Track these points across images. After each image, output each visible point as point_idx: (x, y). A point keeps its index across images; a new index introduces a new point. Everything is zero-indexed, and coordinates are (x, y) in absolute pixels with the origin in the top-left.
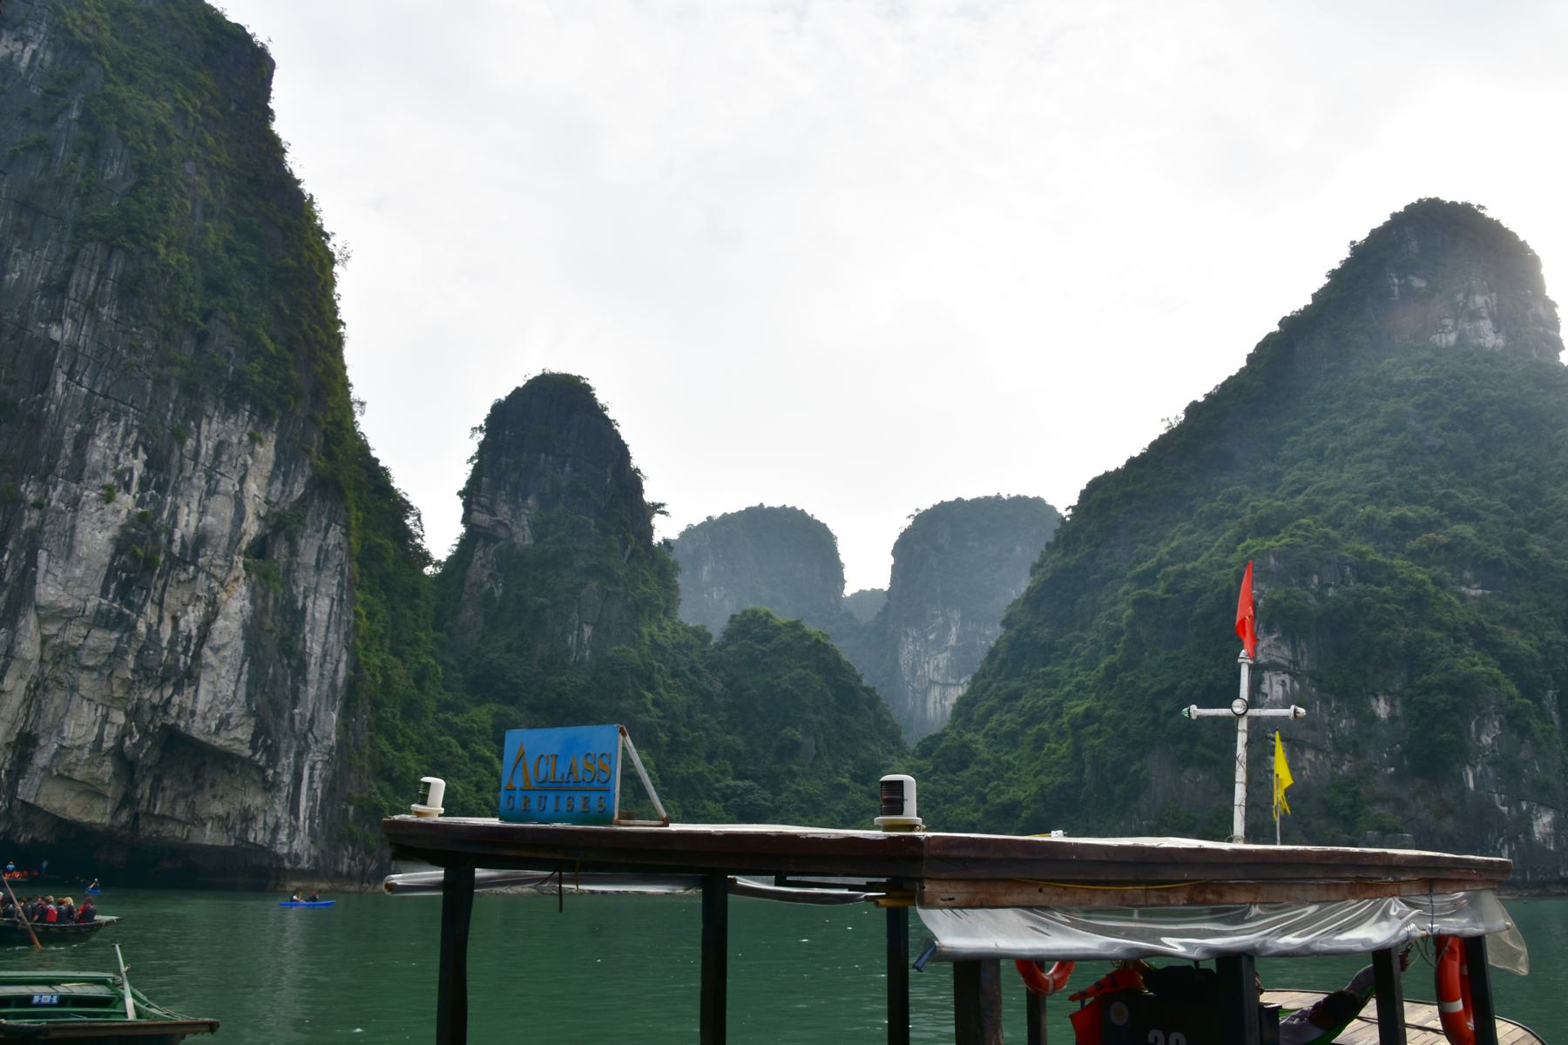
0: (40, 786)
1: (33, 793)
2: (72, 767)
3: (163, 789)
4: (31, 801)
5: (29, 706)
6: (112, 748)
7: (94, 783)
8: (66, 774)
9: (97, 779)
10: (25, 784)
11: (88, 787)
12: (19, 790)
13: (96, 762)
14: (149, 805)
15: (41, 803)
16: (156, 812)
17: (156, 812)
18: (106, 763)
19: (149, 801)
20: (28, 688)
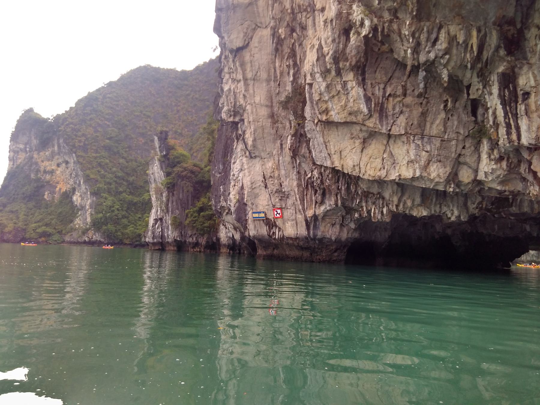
0: (325, 142)
1: (324, 154)
2: (324, 107)
3: (526, 95)
4: (328, 164)
5: (293, 54)
6: (336, 60)
7: (360, 118)
8: (324, 118)
9: (356, 112)
10: (314, 145)
11: (364, 128)
12: (314, 156)
13: (339, 87)
14: (509, 133)
15: (337, 165)
16: (525, 141)
17: (525, 141)
18: (349, 85)
19: (508, 126)
20: (274, 34)
